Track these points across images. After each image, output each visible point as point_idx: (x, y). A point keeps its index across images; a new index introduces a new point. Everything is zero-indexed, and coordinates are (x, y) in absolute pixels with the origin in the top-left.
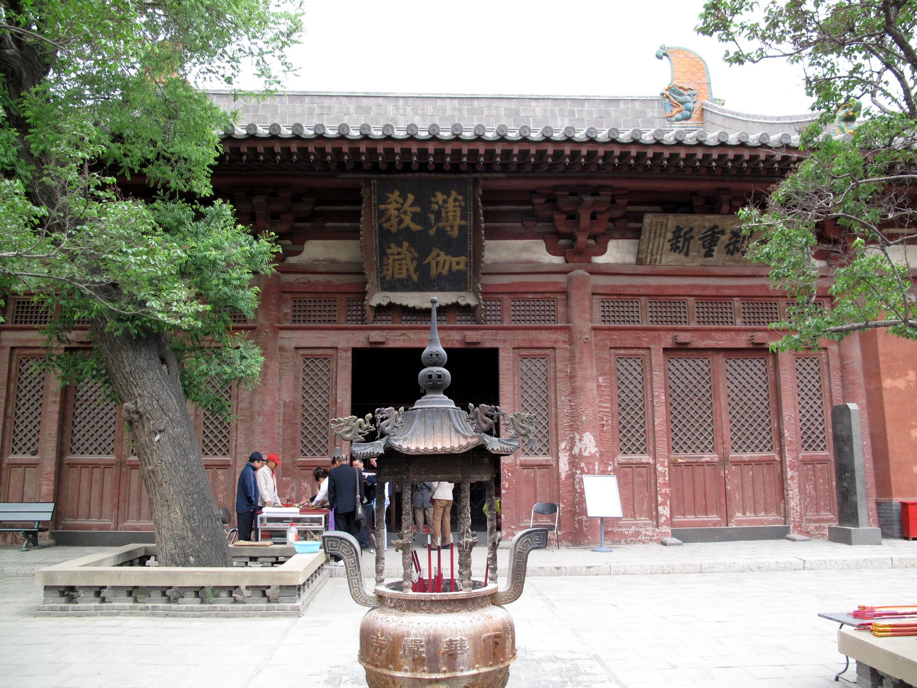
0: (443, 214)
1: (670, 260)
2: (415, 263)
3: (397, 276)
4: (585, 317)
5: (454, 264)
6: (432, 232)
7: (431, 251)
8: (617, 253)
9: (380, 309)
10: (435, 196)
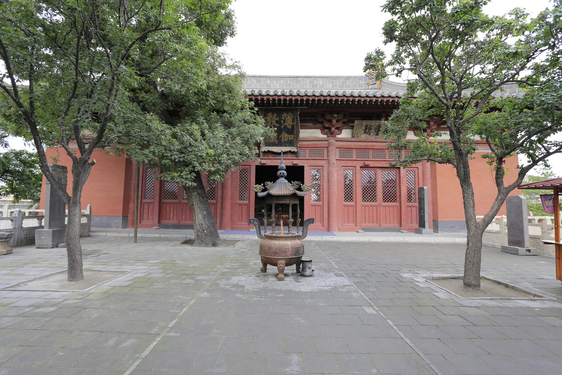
1: (364, 136)
3: (271, 141)
4: (335, 155)
6: (282, 127)
8: (345, 134)
9: (265, 152)
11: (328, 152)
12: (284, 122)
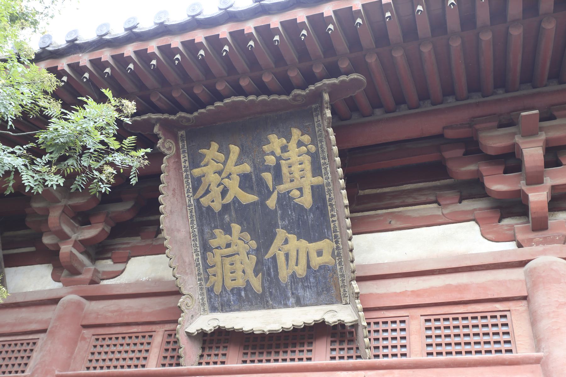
0: (285, 170)
3: (230, 285)
5: (313, 255)
6: (272, 203)
7: (274, 235)
11: (534, 322)
12: (278, 177)
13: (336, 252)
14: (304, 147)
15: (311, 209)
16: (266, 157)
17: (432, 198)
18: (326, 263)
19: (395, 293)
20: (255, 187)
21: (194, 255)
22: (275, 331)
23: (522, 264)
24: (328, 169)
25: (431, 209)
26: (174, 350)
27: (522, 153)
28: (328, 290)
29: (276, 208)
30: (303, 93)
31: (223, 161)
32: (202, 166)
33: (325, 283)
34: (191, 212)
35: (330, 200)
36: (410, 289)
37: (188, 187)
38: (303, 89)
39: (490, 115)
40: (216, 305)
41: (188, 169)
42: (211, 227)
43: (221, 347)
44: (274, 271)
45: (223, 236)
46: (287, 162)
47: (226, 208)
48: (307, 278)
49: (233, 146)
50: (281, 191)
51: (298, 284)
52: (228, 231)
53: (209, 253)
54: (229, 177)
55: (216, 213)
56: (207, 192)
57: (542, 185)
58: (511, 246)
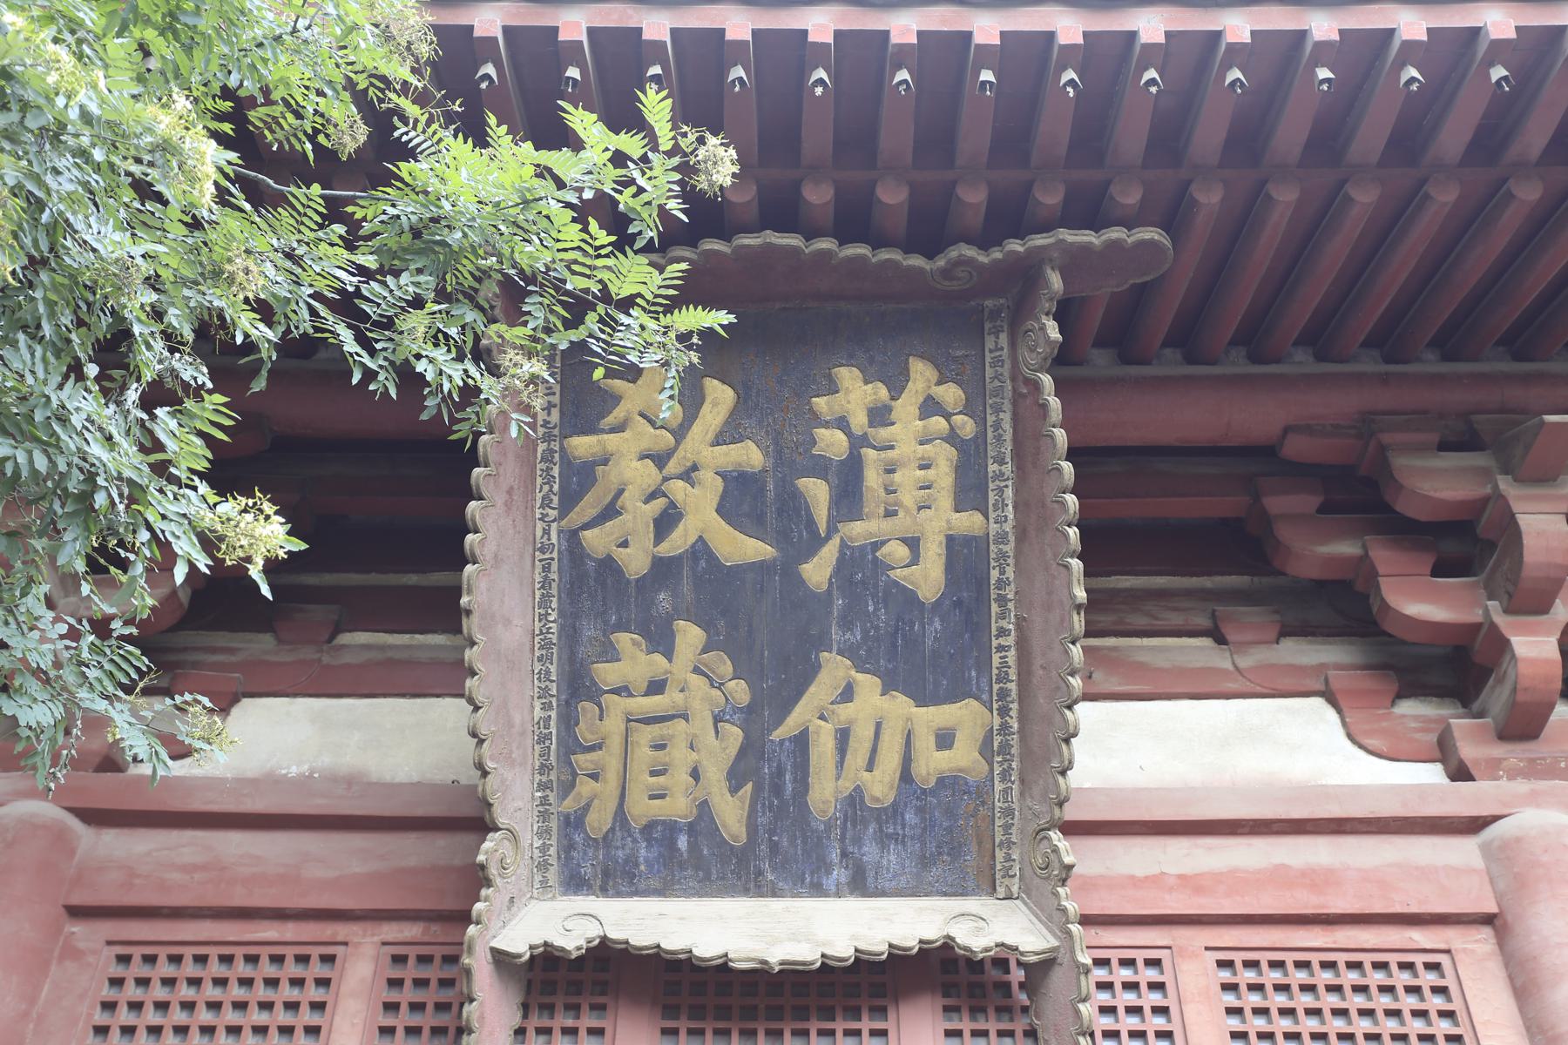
0: (872, 478)
2: (734, 735)
3: (642, 808)
5: (925, 743)
6: (818, 571)
7: (815, 668)
10: (833, 389)
12: (849, 496)
13: (997, 740)
14: (941, 420)
15: (938, 603)
16: (821, 433)
17: (1203, 621)
18: (960, 770)
19: (1132, 877)
20: (771, 515)
21: (538, 705)
22: (804, 963)
23: (1473, 825)
24: (1009, 493)
25: (1197, 652)
26: (442, 1007)
27: (1516, 523)
28: (956, 851)
29: (829, 591)
30: (983, 259)
31: (675, 424)
32: (603, 431)
33: (949, 830)
34: (546, 569)
35: (1001, 584)
36: (1173, 870)
37: (546, 488)
38: (984, 246)
39: (1414, 412)
40: (587, 870)
41: (556, 432)
42: (606, 623)
43: (585, 1008)
44: (795, 780)
45: (642, 657)
46: (883, 454)
47: (663, 569)
48: (895, 812)
49: (716, 382)
50: (851, 539)
51: (866, 828)
52: (661, 641)
53: (587, 705)
54: (689, 474)
55: (628, 581)
56: (610, 512)
57: (1544, 617)
58: (1431, 774)
